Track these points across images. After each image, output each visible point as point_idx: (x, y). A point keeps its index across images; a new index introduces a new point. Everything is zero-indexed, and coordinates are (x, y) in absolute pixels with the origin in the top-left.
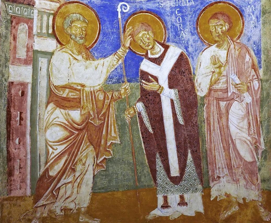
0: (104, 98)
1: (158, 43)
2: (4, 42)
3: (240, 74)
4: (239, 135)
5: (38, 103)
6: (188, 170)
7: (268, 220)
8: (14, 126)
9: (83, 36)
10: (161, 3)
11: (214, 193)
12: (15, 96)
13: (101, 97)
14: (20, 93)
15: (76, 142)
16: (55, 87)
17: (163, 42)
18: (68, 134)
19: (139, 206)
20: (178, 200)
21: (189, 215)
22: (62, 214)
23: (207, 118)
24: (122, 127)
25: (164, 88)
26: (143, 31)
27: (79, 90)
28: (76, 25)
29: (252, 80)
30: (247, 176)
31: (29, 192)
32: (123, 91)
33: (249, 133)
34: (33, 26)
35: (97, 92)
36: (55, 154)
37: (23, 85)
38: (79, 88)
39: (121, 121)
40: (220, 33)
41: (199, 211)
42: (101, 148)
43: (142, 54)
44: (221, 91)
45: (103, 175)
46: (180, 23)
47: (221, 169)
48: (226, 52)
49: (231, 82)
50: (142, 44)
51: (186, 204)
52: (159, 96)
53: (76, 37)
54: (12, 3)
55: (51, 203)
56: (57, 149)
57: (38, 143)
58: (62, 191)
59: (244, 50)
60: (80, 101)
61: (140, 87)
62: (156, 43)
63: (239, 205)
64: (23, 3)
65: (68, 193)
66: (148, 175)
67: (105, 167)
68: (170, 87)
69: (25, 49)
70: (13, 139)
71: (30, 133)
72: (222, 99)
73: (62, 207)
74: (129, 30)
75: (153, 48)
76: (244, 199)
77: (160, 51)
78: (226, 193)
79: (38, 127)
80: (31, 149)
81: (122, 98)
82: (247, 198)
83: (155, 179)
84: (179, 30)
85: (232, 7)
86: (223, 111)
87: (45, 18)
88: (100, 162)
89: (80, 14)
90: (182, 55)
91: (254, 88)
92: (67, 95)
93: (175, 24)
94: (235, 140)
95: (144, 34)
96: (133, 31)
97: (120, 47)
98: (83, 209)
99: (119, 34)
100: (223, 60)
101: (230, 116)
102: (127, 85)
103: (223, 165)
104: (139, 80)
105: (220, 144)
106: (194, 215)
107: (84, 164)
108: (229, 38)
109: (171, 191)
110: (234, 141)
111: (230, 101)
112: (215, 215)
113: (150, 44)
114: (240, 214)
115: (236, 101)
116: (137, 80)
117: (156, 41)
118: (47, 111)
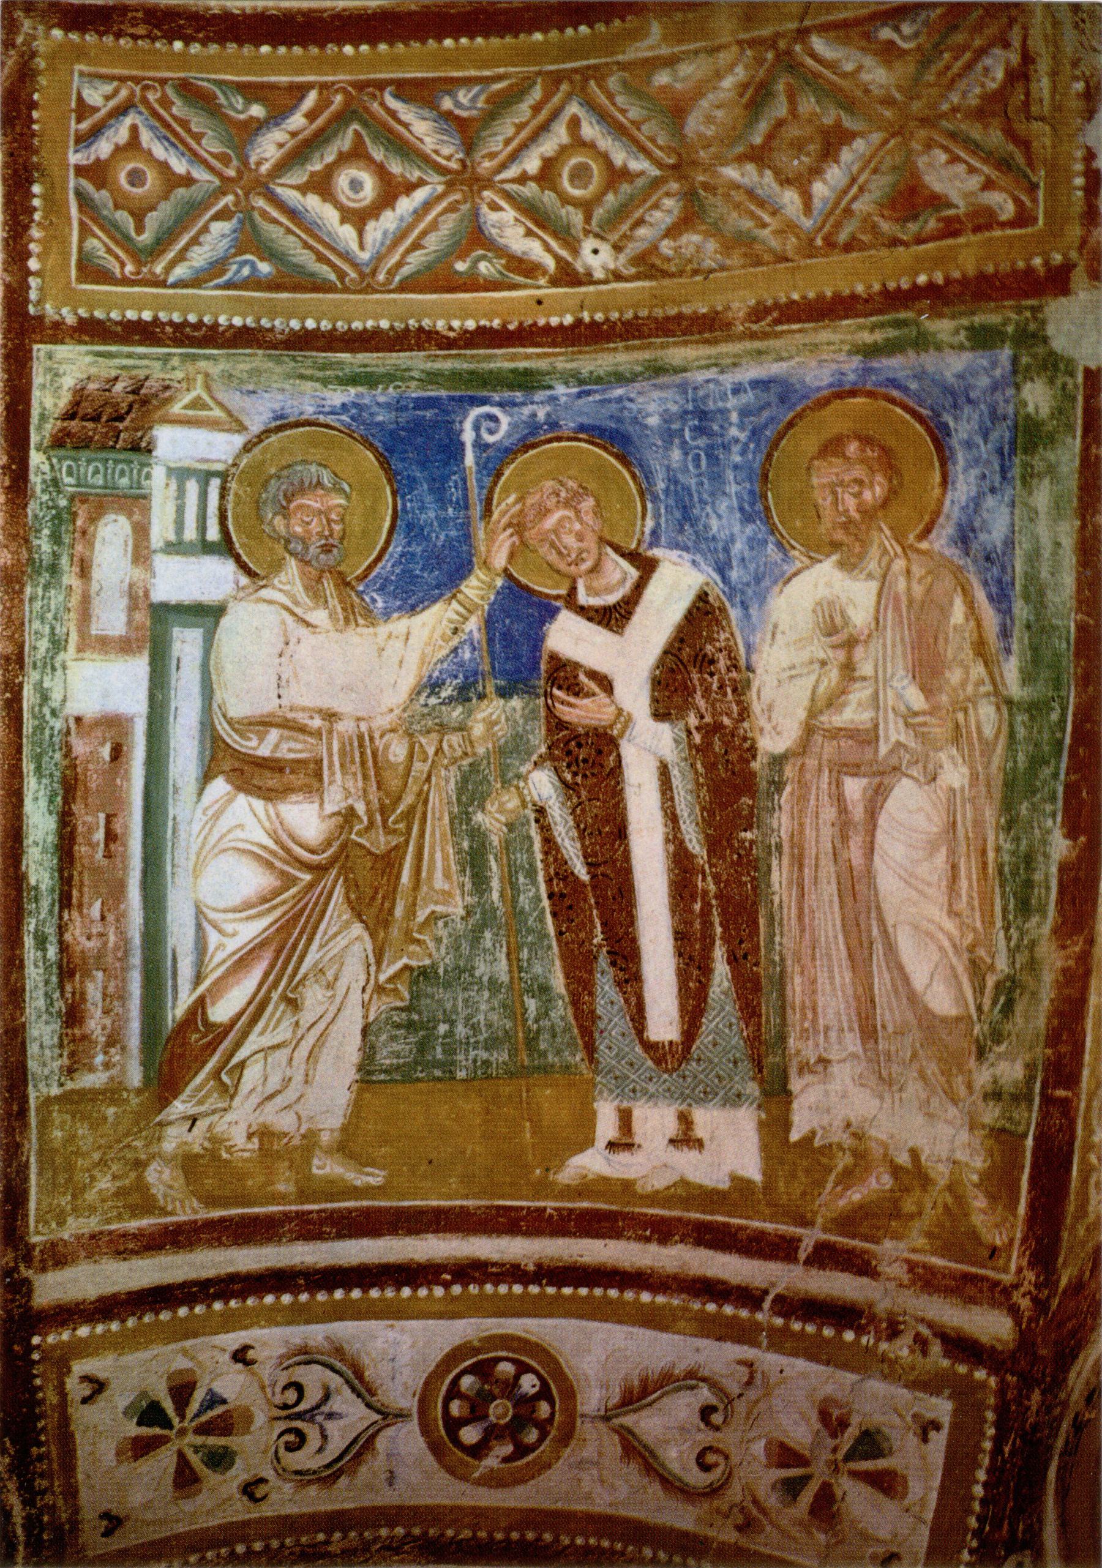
0: (411, 756)
1: (617, 549)
6: (710, 1023)
8: (86, 862)
10: (631, 400)
13: (398, 751)
14: (106, 752)
15: (302, 912)
16: (230, 722)
18: (278, 883)
20: (671, 1126)
22: (250, 1146)
27: (318, 734)
29: (973, 700)
32: (478, 730)
33: (950, 905)
38: (317, 723)
40: (854, 514)
43: (554, 592)
45: (398, 1026)
47: (833, 1035)
48: (874, 585)
49: (890, 703)
50: (553, 557)
51: (699, 1144)
53: (306, 548)
55: (214, 1112)
58: (252, 1075)
60: (321, 769)
61: (543, 713)
62: (609, 550)
63: (896, 1171)
65: (274, 1083)
69: (124, 602)
70: (80, 906)
72: (855, 770)
75: (595, 569)
77: (624, 580)
83: (590, 1049)
86: (858, 813)
88: (391, 980)
90: (702, 596)
91: (979, 732)
92: (277, 746)
93: (680, 476)
95: (561, 520)
96: (521, 511)
98: (325, 1138)
100: (860, 616)
101: (880, 836)
103: (844, 1018)
106: (725, 1185)
107: (330, 986)
108: (888, 533)
109: (645, 1092)
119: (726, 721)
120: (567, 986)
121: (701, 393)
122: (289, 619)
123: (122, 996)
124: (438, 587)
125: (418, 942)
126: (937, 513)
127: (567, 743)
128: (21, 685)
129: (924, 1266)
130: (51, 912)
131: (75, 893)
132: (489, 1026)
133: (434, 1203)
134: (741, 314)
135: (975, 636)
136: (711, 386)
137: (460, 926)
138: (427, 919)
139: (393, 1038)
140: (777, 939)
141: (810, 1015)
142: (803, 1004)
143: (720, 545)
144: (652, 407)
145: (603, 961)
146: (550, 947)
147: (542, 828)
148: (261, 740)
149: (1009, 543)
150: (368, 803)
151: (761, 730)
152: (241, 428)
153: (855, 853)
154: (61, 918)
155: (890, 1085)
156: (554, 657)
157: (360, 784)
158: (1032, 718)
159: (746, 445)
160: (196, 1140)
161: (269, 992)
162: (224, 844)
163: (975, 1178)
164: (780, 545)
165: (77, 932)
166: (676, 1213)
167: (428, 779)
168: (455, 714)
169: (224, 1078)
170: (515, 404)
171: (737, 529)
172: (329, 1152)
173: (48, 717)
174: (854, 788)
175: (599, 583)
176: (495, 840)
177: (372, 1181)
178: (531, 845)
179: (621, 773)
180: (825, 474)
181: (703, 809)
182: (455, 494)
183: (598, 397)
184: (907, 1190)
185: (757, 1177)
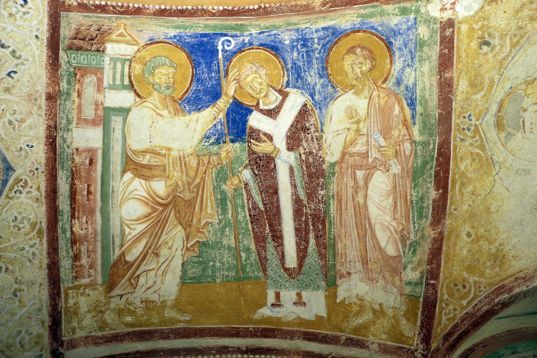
0: (198, 164)
1: (274, 88)
2: (65, 100)
3: (386, 133)
4: (380, 218)
5: (111, 173)
6: (308, 260)
7: (410, 336)
8: (80, 202)
9: (169, 85)
10: (279, 35)
11: (342, 293)
12: (81, 165)
13: (193, 162)
14: (87, 162)
15: (159, 221)
16: (132, 151)
17: (280, 87)
18: (150, 211)
19: (243, 302)
20: (294, 298)
21: (307, 318)
22: (142, 306)
23: (338, 193)
24: (222, 202)
25: (281, 149)
26: (253, 74)
27: (164, 155)
28: (159, 72)
29: (402, 141)
30: (388, 275)
31: (100, 279)
32: (223, 155)
33: (394, 216)
34: (103, 78)
35: (188, 157)
36: (133, 235)
37: (91, 151)
38: (164, 152)
39: (221, 194)
40: (360, 75)
41: (321, 315)
42: (193, 229)
43: (251, 104)
44: (358, 156)
45: (195, 263)
46: (304, 62)
47: (352, 264)
48: (367, 101)
49: (373, 143)
50: (251, 91)
51: (304, 304)
52: (273, 159)
53: (160, 87)
54: (75, 52)
55: (129, 293)
56: (135, 229)
57: (111, 221)
58: (142, 280)
59: (393, 99)
61: (247, 148)
62: (271, 89)
63: (374, 312)
64: (90, 50)
65: (150, 283)
66: (256, 263)
67: (198, 252)
68: (289, 149)
69: (94, 107)
70: (78, 218)
71: (101, 209)
72: (360, 167)
73: (142, 298)
74: (232, 74)
76: (381, 305)
78: (357, 296)
79: (110, 202)
80: (101, 229)
81: (222, 164)
82: (385, 304)
83: (265, 270)
84: (302, 70)
85: (375, 37)
86: (361, 183)
87: (119, 65)
88: (191, 246)
89: (165, 57)
90: (305, 105)
92: (149, 160)
93: (297, 62)
94: (374, 224)
95: (254, 77)
96: (239, 74)
97: (220, 96)
98: (169, 303)
99: (219, 79)
102: (230, 146)
103: (356, 257)
104: (245, 139)
105: (353, 229)
106: (313, 319)
107: (170, 248)
108: (372, 82)
109: (285, 285)
110: (373, 225)
111: (371, 169)
112: (342, 321)
113: (262, 91)
114: (374, 323)
115: (379, 170)
116: (244, 139)
117: (271, 87)
118: (122, 182)
119: (314, 151)
120: (256, 248)
121: (304, 32)
122: (154, 113)
123: (94, 251)
124: (209, 102)
125: (202, 232)
126: (389, 74)
127: (256, 160)
128: (56, 136)
129: (384, 345)
130: (67, 220)
131: (76, 213)
132: (228, 263)
133: (210, 326)
134: (318, 4)
135: (403, 119)
136: (308, 29)
137: (217, 226)
138: (205, 224)
139: (193, 267)
140: (332, 230)
141: (344, 257)
142: (341, 254)
143: (311, 87)
144: (286, 38)
145: (270, 239)
146: (250, 234)
147: (247, 190)
148: (144, 158)
149: (415, 85)
150: (183, 181)
151: (327, 153)
152: (137, 44)
153: (360, 199)
154: (71, 222)
155: (372, 281)
156: (251, 128)
157: (180, 174)
158: (423, 148)
159: (321, 50)
160: (122, 303)
161: (148, 250)
162: (131, 196)
163: (402, 313)
164: (333, 86)
165: (77, 228)
166: (296, 329)
167: (205, 173)
168: (215, 149)
169: (132, 281)
170: (237, 36)
171: (317, 80)
172: (171, 308)
173: (66, 148)
174: (360, 174)
175: (267, 101)
176: (229, 194)
177: (186, 318)
178: (243, 197)
179: (276, 170)
180: (349, 60)
181: (306, 183)
182: (215, 68)
183: (267, 34)
184: (378, 318)
185: (325, 315)
